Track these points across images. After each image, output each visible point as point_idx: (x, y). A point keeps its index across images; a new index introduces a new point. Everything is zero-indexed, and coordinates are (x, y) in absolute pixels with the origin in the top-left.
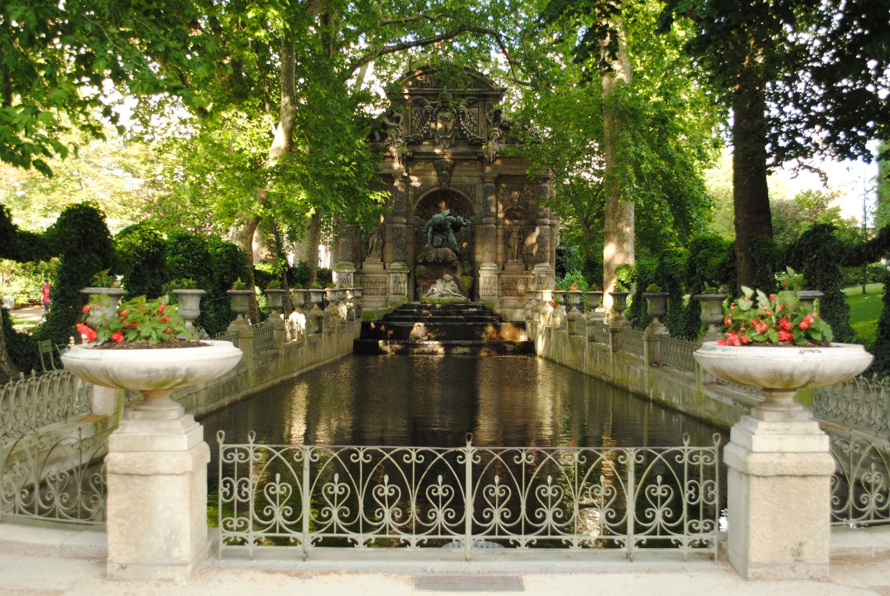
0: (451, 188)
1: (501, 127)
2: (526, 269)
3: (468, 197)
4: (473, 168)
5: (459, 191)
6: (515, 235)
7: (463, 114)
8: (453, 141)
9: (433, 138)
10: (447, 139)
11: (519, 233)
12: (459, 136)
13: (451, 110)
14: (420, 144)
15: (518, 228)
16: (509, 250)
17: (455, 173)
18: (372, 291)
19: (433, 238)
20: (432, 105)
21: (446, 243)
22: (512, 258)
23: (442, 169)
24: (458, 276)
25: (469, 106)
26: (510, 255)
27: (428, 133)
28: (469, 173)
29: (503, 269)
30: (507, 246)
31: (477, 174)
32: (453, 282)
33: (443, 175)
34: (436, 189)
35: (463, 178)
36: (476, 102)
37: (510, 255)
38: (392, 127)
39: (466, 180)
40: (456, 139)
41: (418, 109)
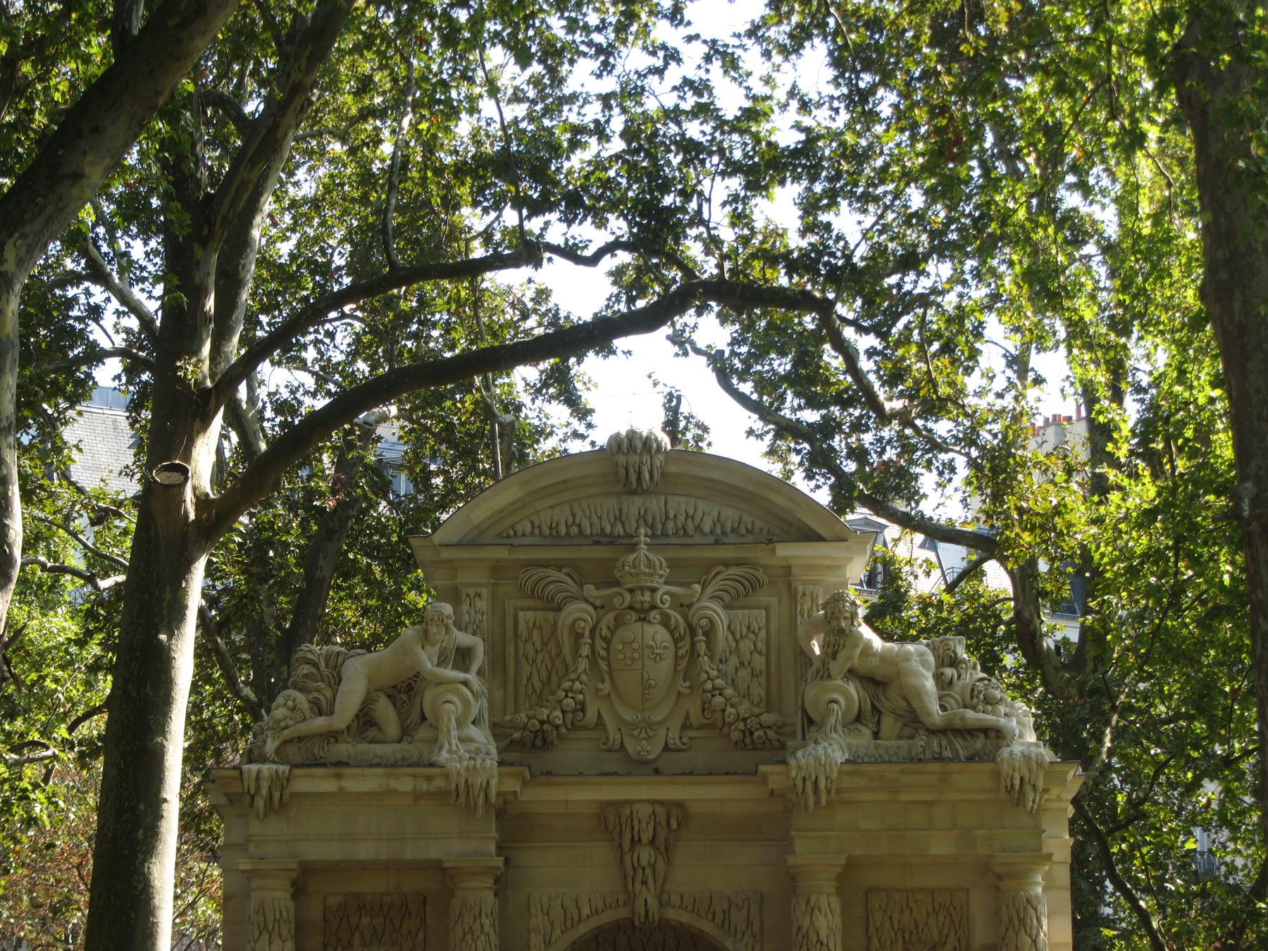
1: (852, 673)
7: (710, 633)
8: (674, 735)
12: (696, 717)
13: (665, 622)
14: (546, 745)
23: (635, 842)
27: (582, 707)
38: (441, 682)
40: (685, 726)
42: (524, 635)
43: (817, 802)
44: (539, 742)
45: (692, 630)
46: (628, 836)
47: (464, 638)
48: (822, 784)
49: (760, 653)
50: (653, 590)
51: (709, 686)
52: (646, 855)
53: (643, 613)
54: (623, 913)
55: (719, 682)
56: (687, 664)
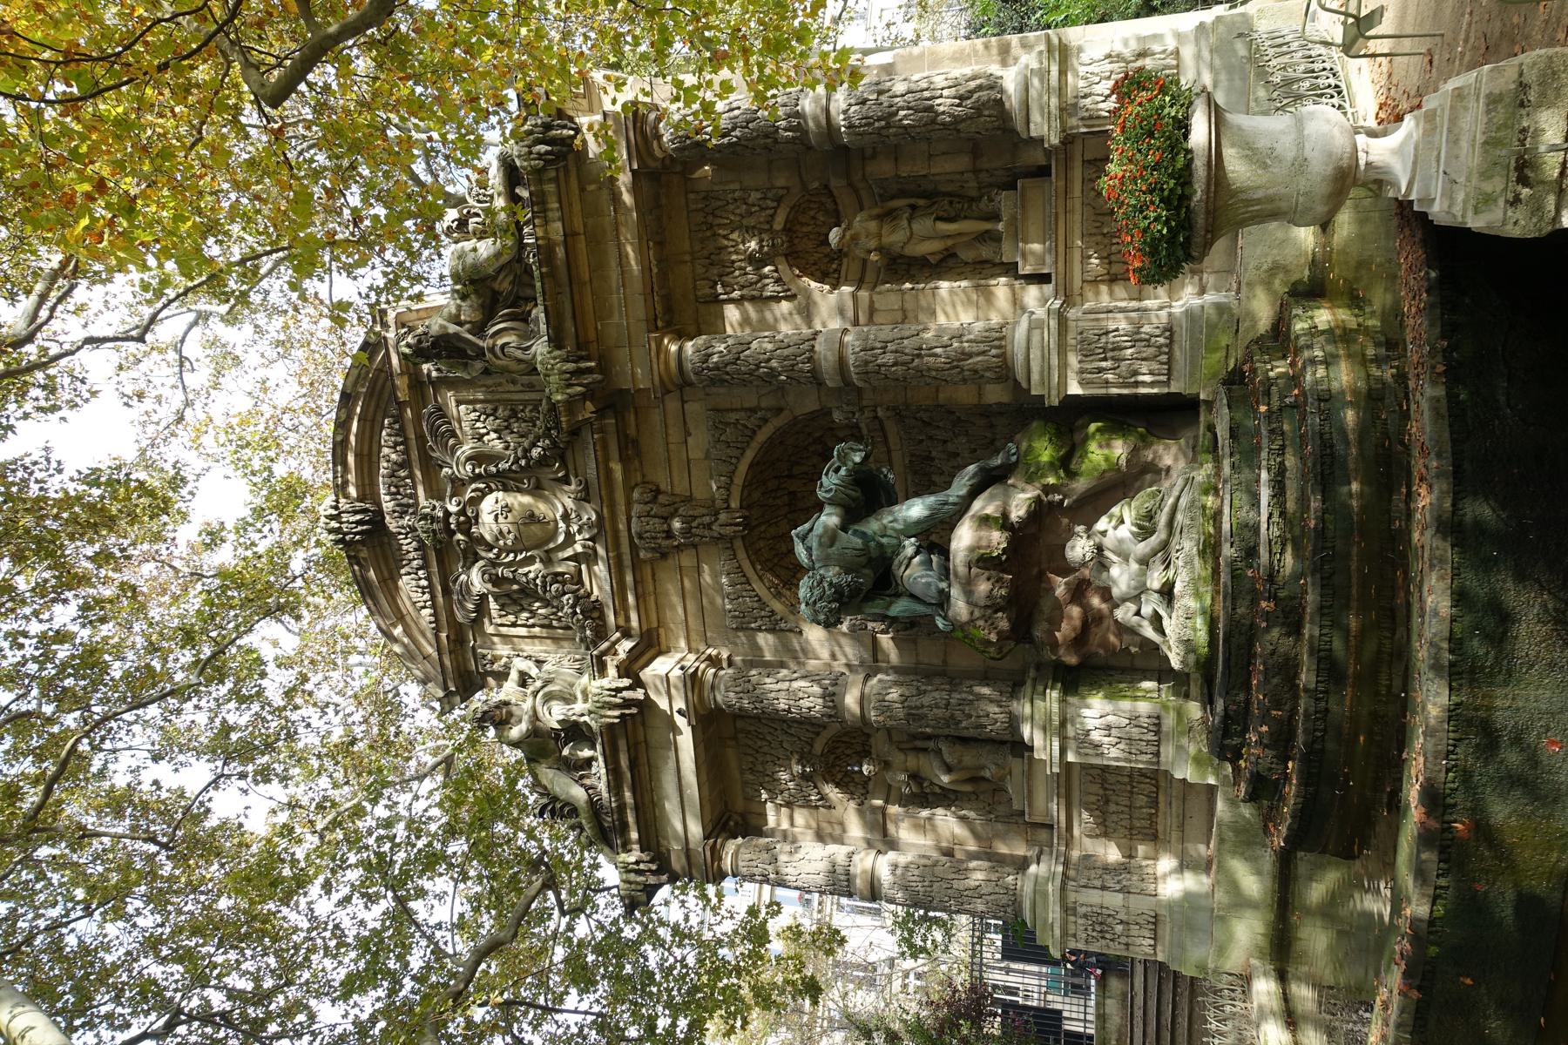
0: (734, 504)
1: (479, 329)
2: (1043, 172)
3: (762, 436)
4: (656, 417)
5: (743, 468)
6: (895, 237)
7: (477, 458)
9: (575, 558)
10: (566, 517)
11: (888, 216)
13: (476, 501)
15: (863, 224)
16: (967, 255)
17: (681, 488)
18: (1141, 800)
19: (912, 596)
20: (468, 567)
21: (934, 536)
22: (995, 238)
23: (669, 534)
24: (1081, 485)
25: (447, 436)
26: (985, 252)
28: (675, 435)
29: (1042, 279)
30: (944, 265)
31: (672, 404)
32: (1103, 524)
33: (686, 532)
34: (742, 554)
35: (696, 454)
36: (441, 412)
37: (985, 252)
39: (699, 441)
41: (493, 605)
42: (511, 618)
43: (589, 371)
44: (596, 615)
45: (477, 478)
46: (665, 543)
47: (514, 675)
48: (570, 366)
49: (495, 410)
50: (447, 514)
51: (523, 462)
52: (677, 524)
53: (469, 521)
54: (738, 544)
55: (520, 453)
56: (506, 481)
